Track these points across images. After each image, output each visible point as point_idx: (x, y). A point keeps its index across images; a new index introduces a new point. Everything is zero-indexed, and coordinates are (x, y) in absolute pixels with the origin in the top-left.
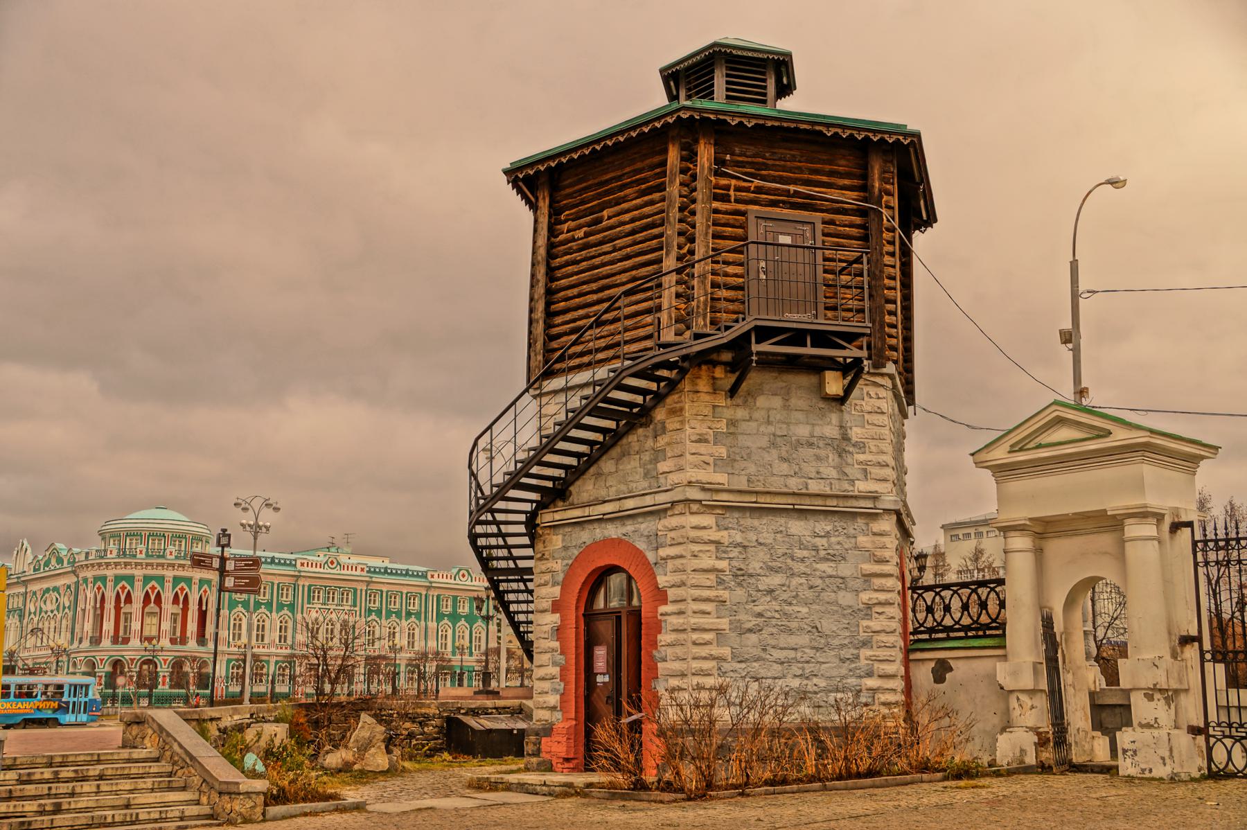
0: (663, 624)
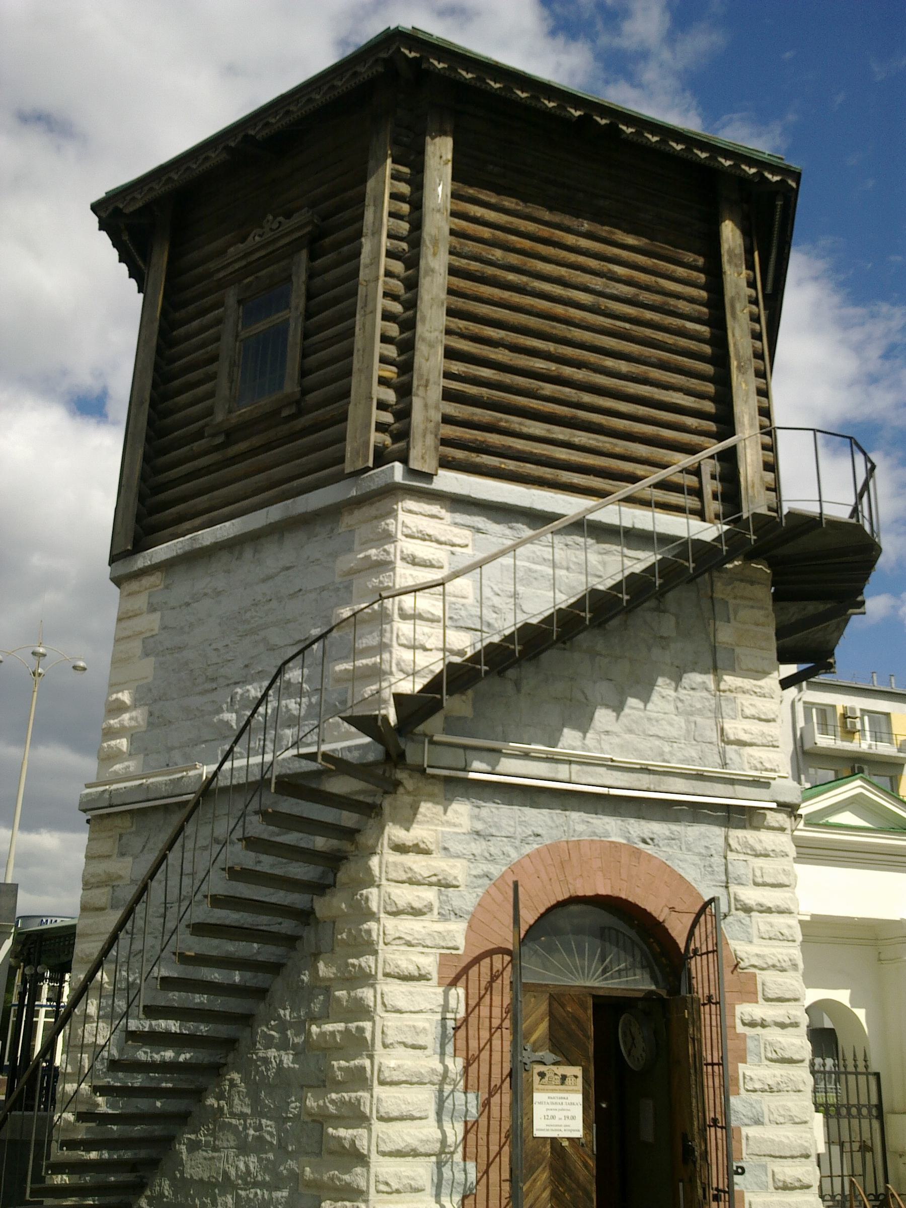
0: (750, 1044)
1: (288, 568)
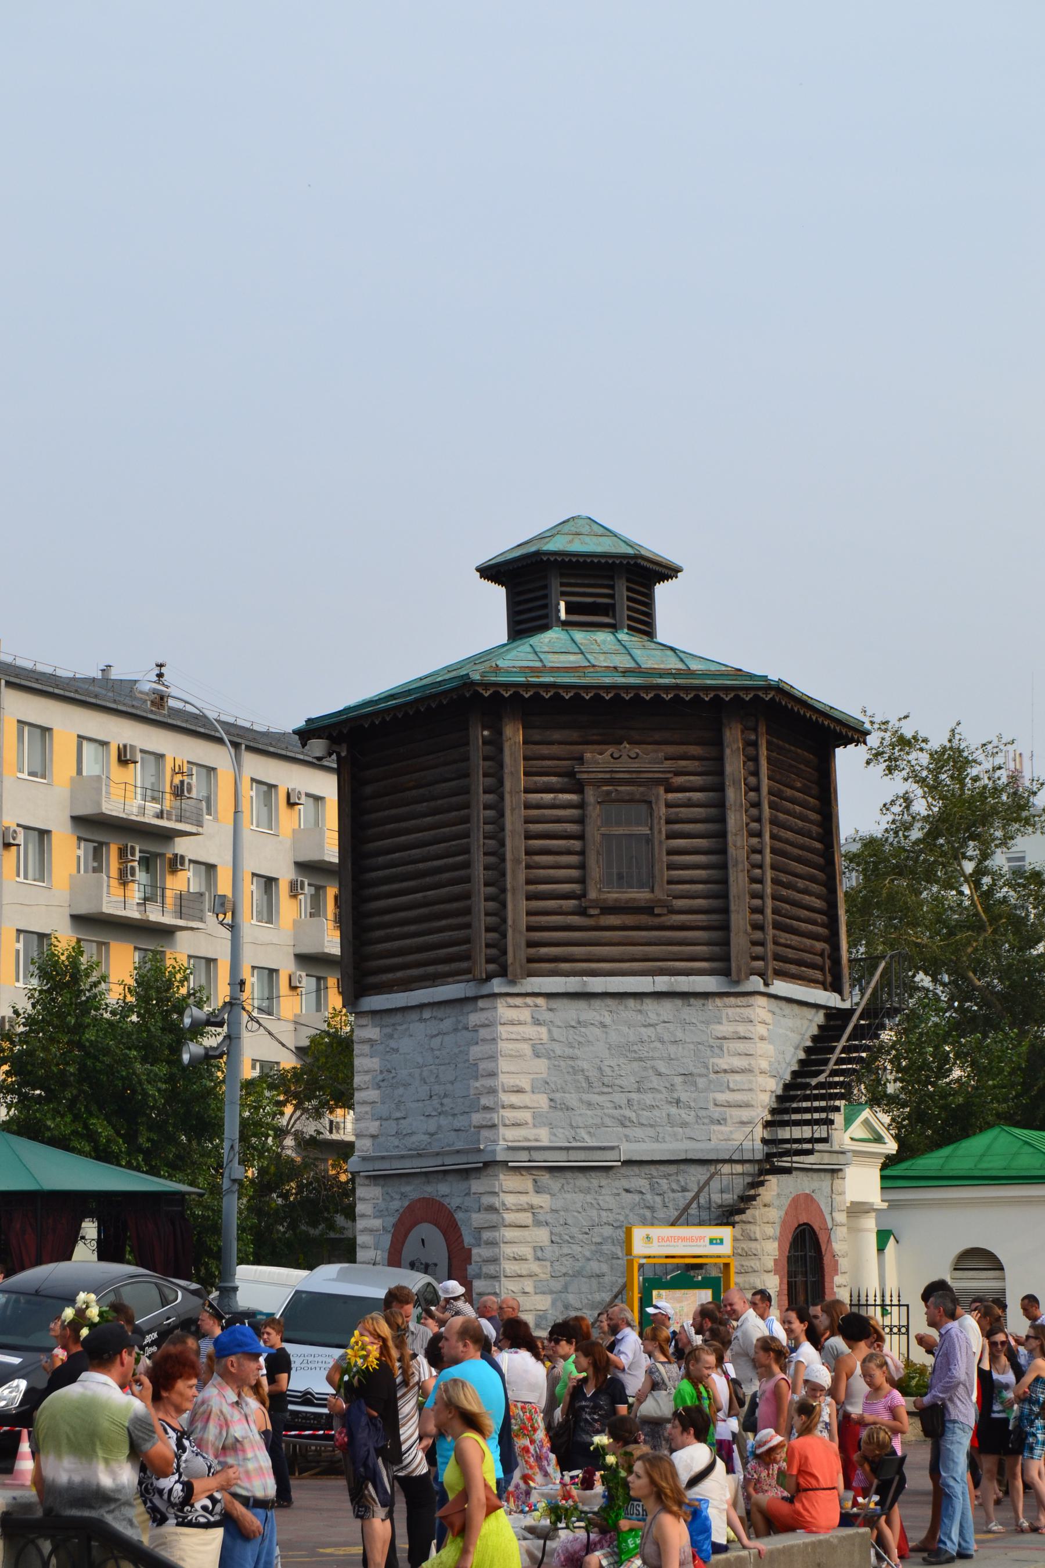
1: (665, 1022)
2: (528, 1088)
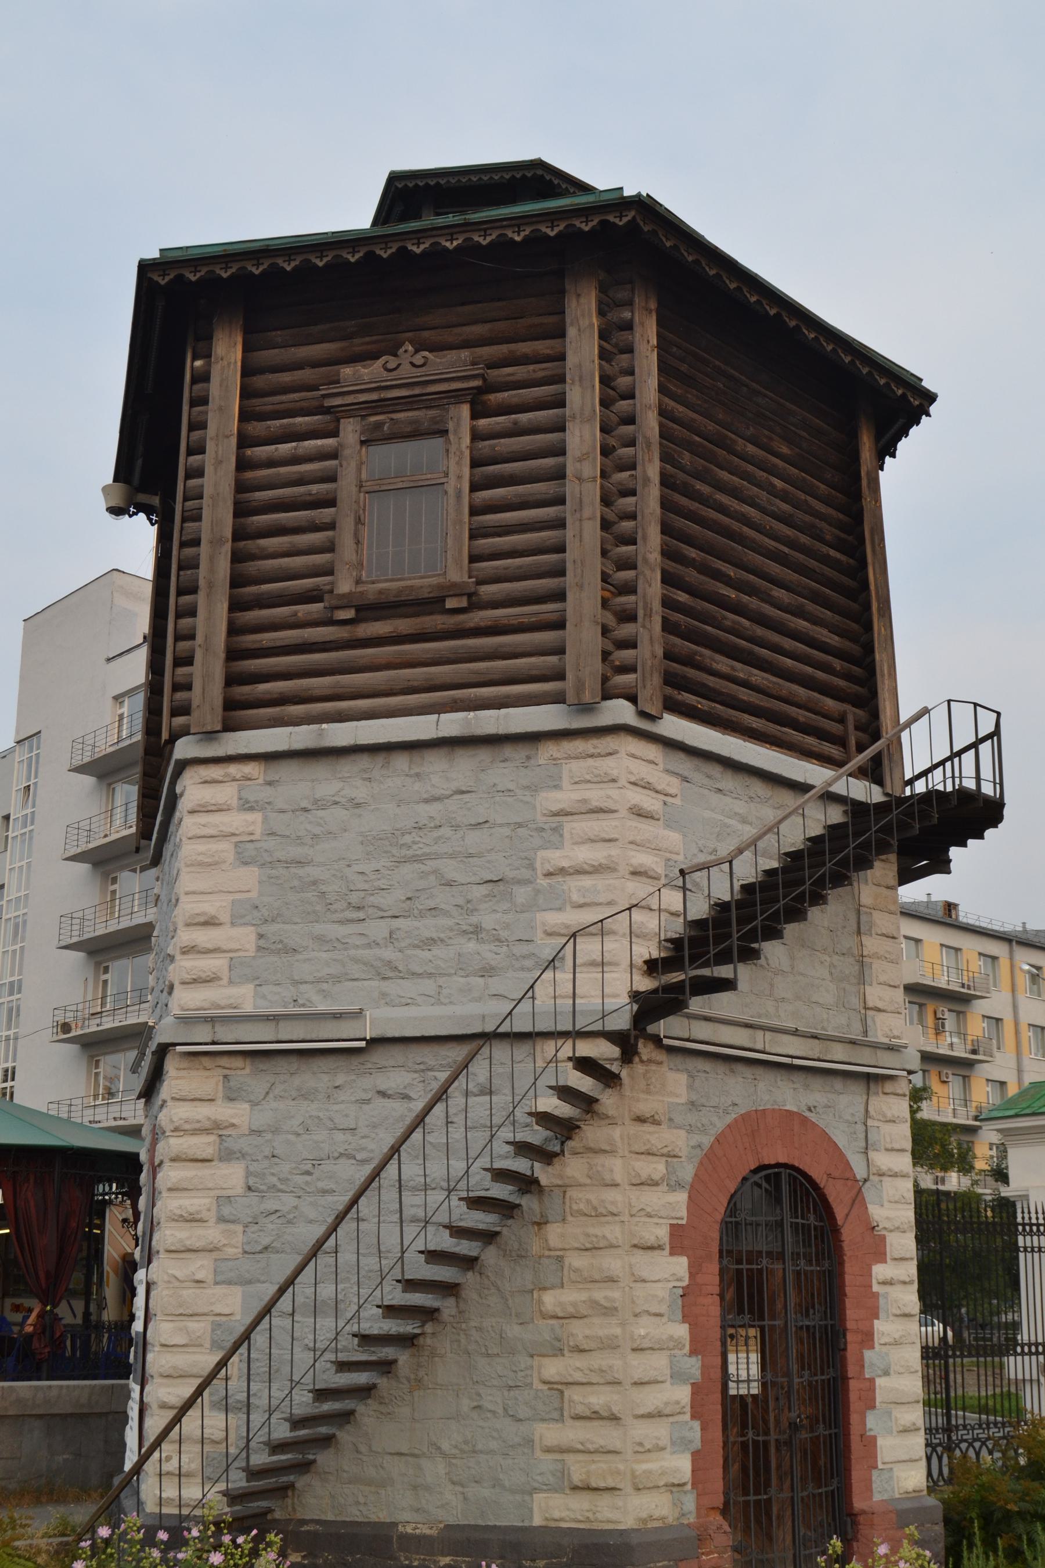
0: (882, 1301)
1: (463, 792)
2: (225, 917)
